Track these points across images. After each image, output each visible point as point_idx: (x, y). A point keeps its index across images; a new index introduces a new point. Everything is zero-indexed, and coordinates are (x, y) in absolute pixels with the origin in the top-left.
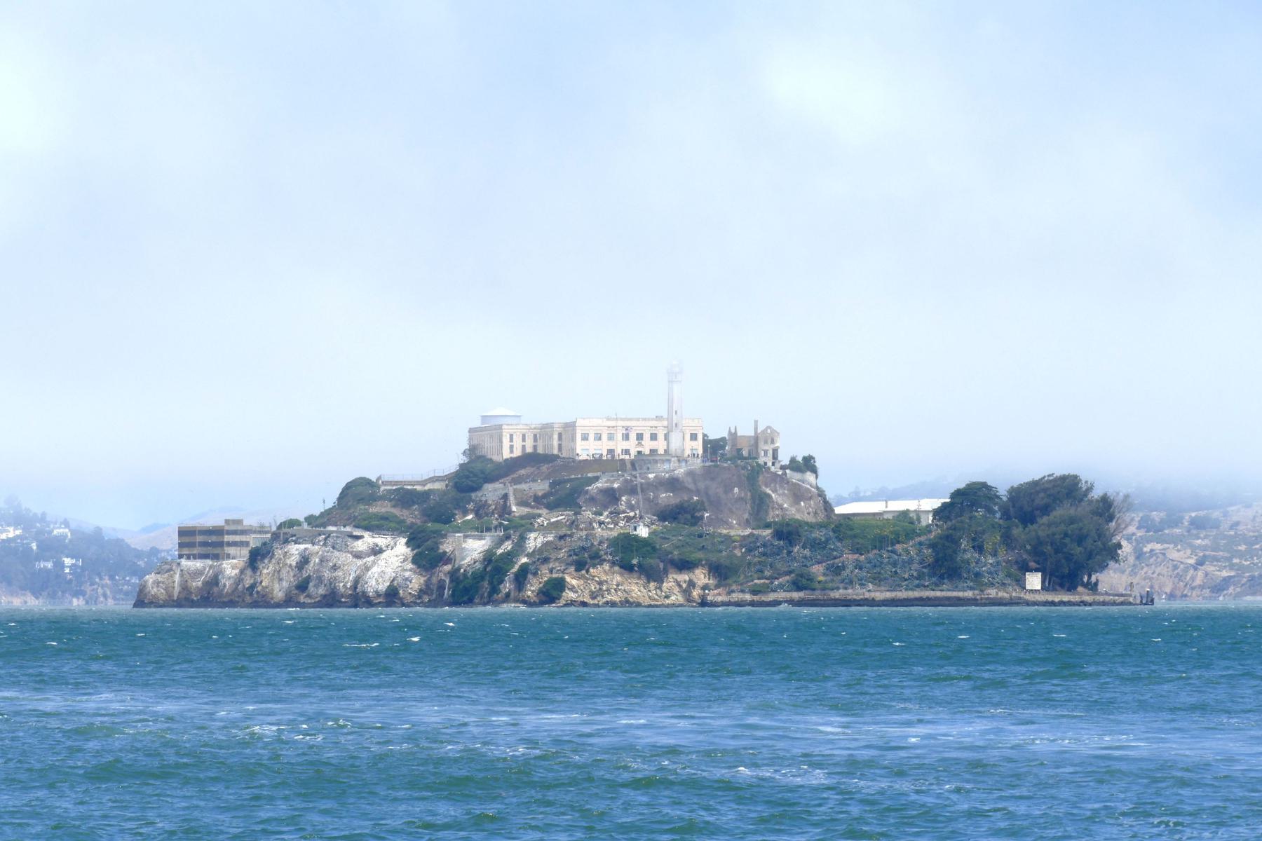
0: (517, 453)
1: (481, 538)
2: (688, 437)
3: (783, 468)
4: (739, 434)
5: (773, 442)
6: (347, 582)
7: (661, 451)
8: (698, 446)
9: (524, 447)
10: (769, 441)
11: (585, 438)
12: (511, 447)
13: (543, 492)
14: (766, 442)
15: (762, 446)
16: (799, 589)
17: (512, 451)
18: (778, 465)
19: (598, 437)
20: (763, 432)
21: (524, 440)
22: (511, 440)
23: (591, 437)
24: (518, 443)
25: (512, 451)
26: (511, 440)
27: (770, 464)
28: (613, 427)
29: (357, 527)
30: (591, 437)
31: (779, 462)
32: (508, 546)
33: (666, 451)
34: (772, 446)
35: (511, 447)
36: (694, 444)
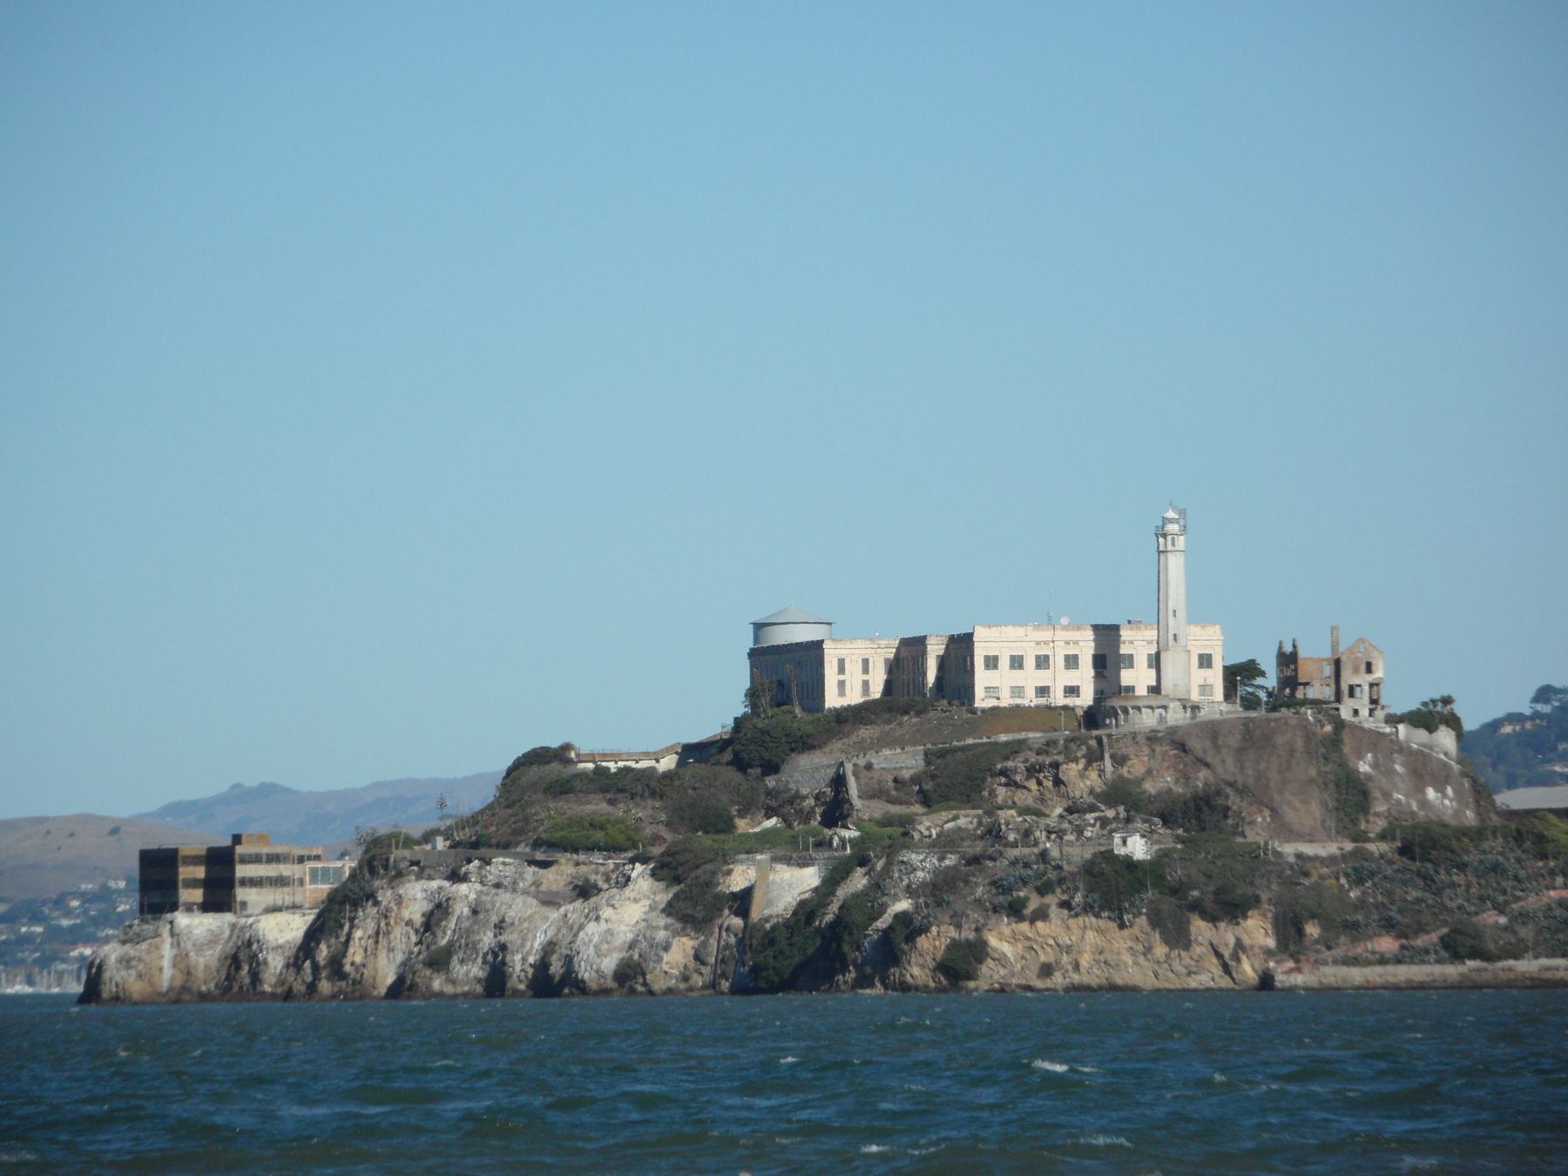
0: (854, 697)
1: (804, 863)
2: (1195, 661)
3: (1393, 720)
4: (1302, 654)
5: (1369, 668)
6: (529, 953)
7: (1141, 691)
8: (1216, 677)
9: (866, 684)
10: (1363, 667)
11: (992, 663)
12: (842, 684)
13: (912, 772)
14: (1356, 671)
15: (1348, 678)
16: (1457, 957)
17: (842, 693)
18: (1380, 714)
19: (1017, 662)
20: (1350, 650)
21: (866, 670)
22: (841, 670)
23: (1004, 662)
24: (854, 676)
25: (842, 693)
26: (841, 670)
27: (1364, 712)
28: (1046, 643)
29: (537, 845)
30: (1004, 662)
31: (1383, 708)
32: (858, 881)
33: (1155, 690)
34: (1370, 678)
35: (842, 684)
36: (1205, 672)
